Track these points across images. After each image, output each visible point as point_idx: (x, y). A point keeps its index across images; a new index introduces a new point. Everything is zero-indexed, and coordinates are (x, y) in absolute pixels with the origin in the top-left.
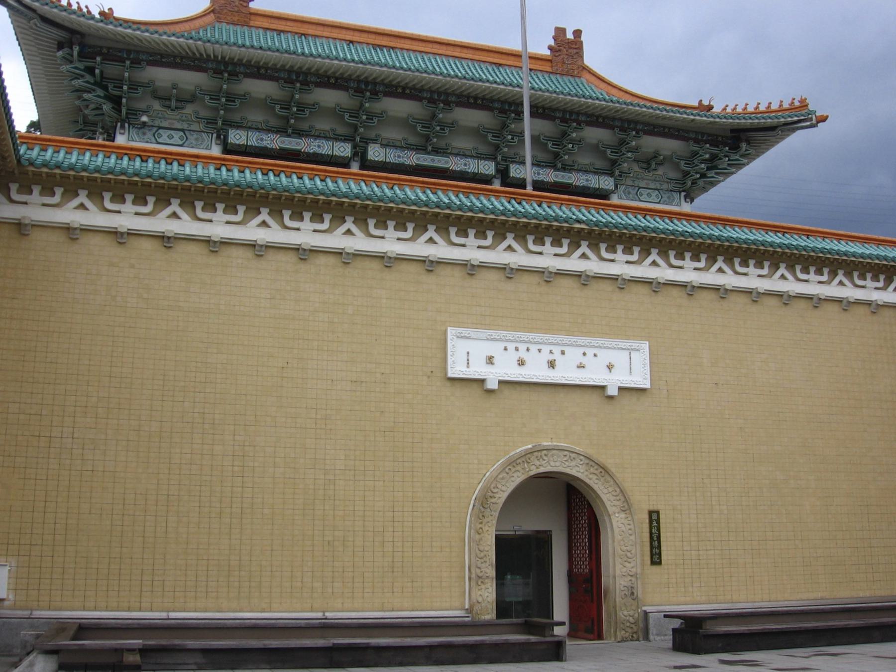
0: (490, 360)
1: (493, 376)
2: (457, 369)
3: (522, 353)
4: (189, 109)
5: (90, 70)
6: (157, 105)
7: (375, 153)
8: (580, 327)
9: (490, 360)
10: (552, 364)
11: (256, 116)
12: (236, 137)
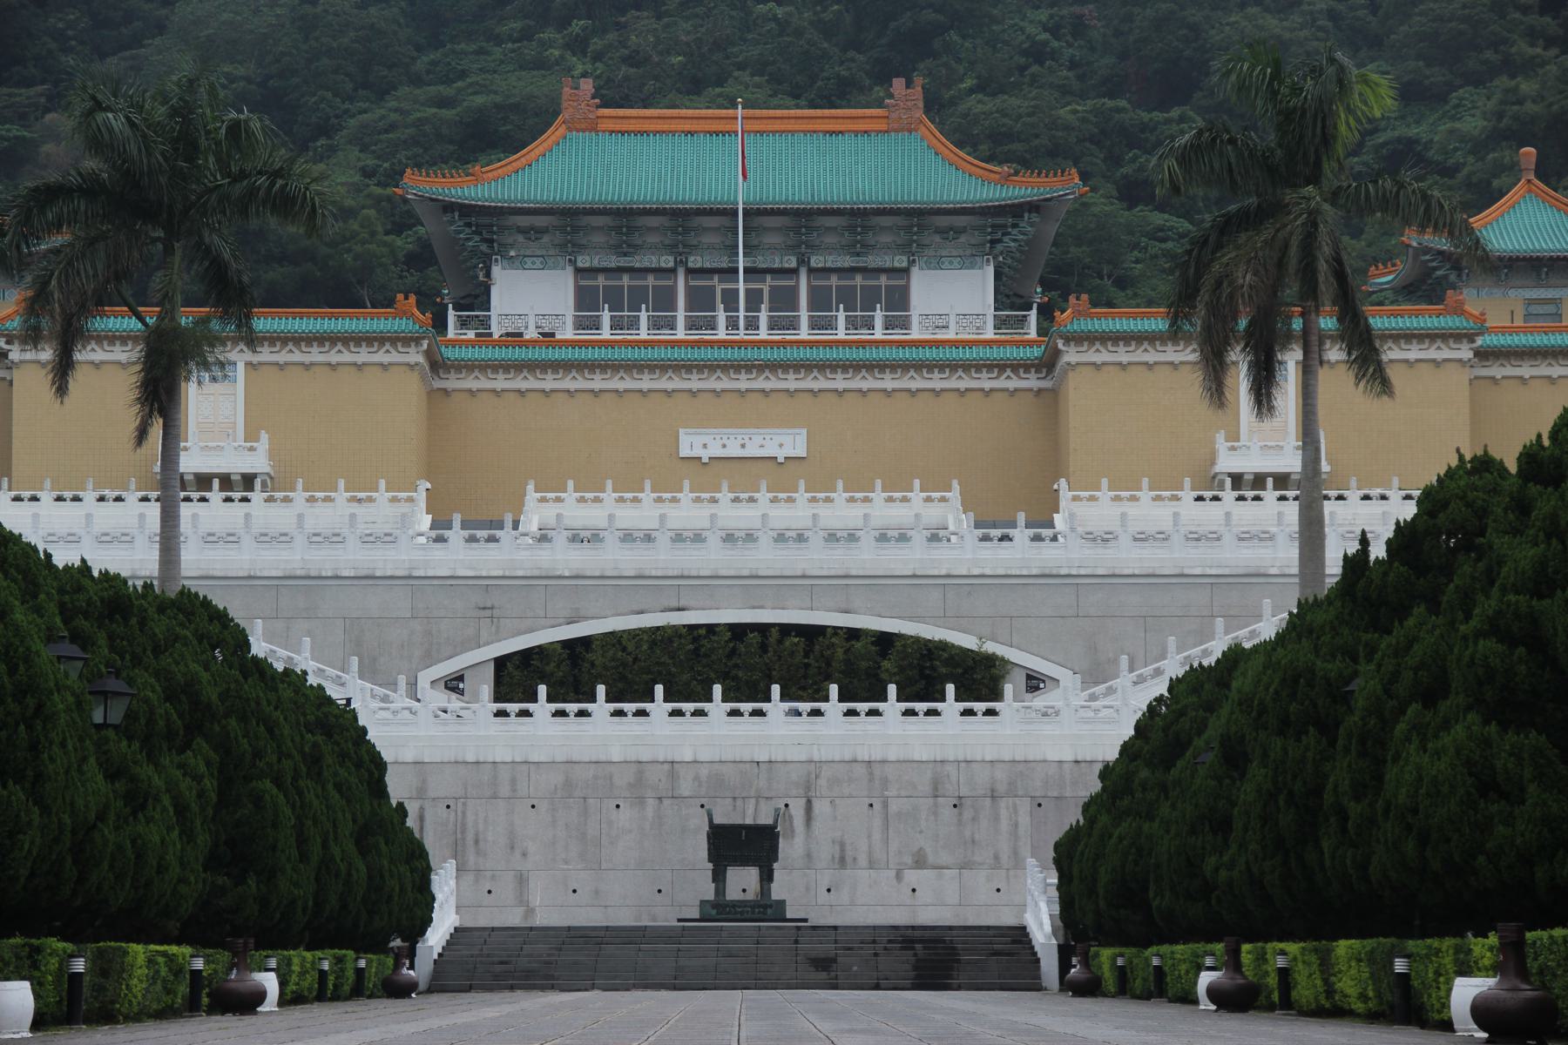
0: (705, 446)
1: (705, 456)
2: (685, 452)
3: (725, 441)
4: (546, 239)
5: (469, 225)
6: (520, 238)
7: (695, 261)
8: (762, 422)
9: (705, 446)
10: (743, 446)
11: (598, 239)
12: (584, 261)
